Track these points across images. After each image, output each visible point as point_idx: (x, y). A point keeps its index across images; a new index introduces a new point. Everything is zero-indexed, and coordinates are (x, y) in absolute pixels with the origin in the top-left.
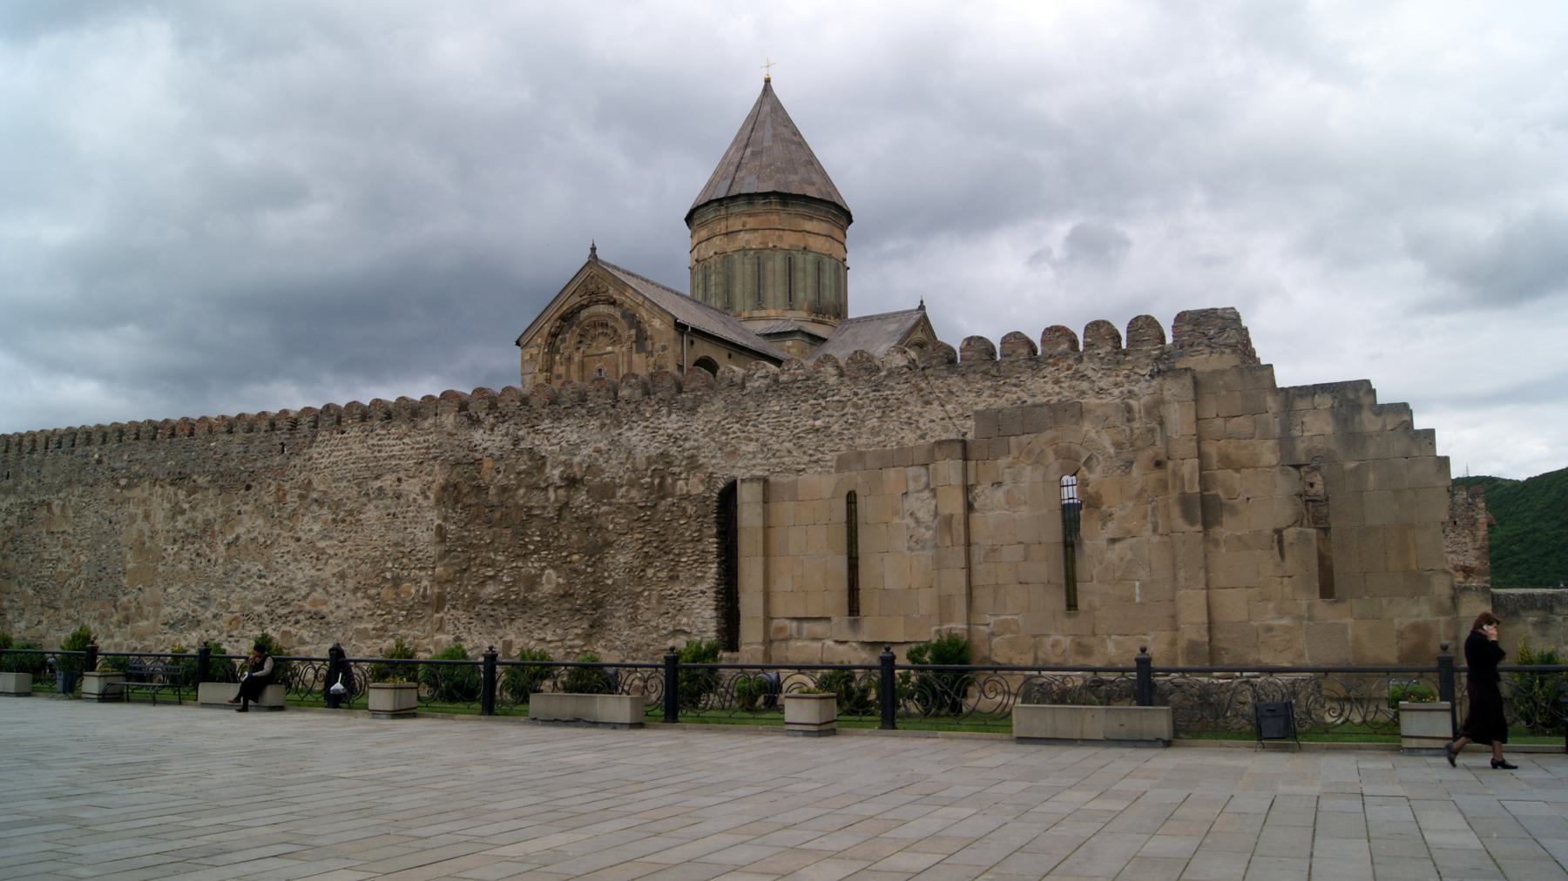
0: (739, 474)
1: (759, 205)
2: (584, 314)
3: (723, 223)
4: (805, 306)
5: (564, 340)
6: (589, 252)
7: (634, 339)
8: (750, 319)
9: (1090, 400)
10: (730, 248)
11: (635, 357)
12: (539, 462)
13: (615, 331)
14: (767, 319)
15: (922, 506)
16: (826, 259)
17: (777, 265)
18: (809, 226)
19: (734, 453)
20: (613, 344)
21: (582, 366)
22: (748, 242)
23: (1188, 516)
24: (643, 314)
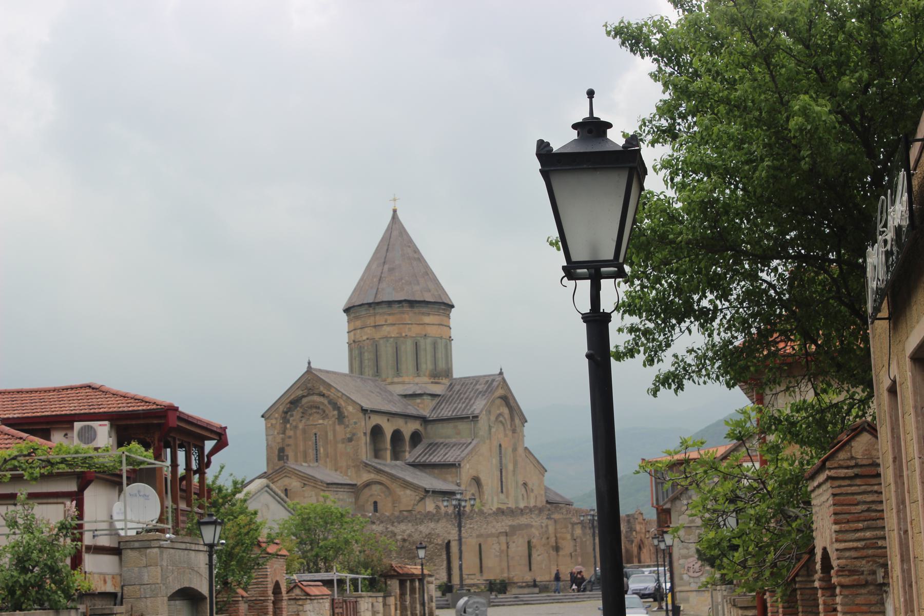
0: (451, 538)
1: (396, 308)
2: (304, 401)
3: (372, 318)
4: (427, 373)
5: (292, 416)
6: (307, 365)
7: (337, 417)
8: (392, 383)
9: (534, 523)
10: (377, 336)
11: (338, 428)
12: (394, 535)
13: (324, 412)
14: (403, 383)
15: (496, 547)
16: (439, 341)
17: (407, 348)
18: (427, 319)
19: (449, 533)
20: (323, 419)
21: (304, 431)
22: (389, 332)
23: (553, 550)
24: (342, 403)
